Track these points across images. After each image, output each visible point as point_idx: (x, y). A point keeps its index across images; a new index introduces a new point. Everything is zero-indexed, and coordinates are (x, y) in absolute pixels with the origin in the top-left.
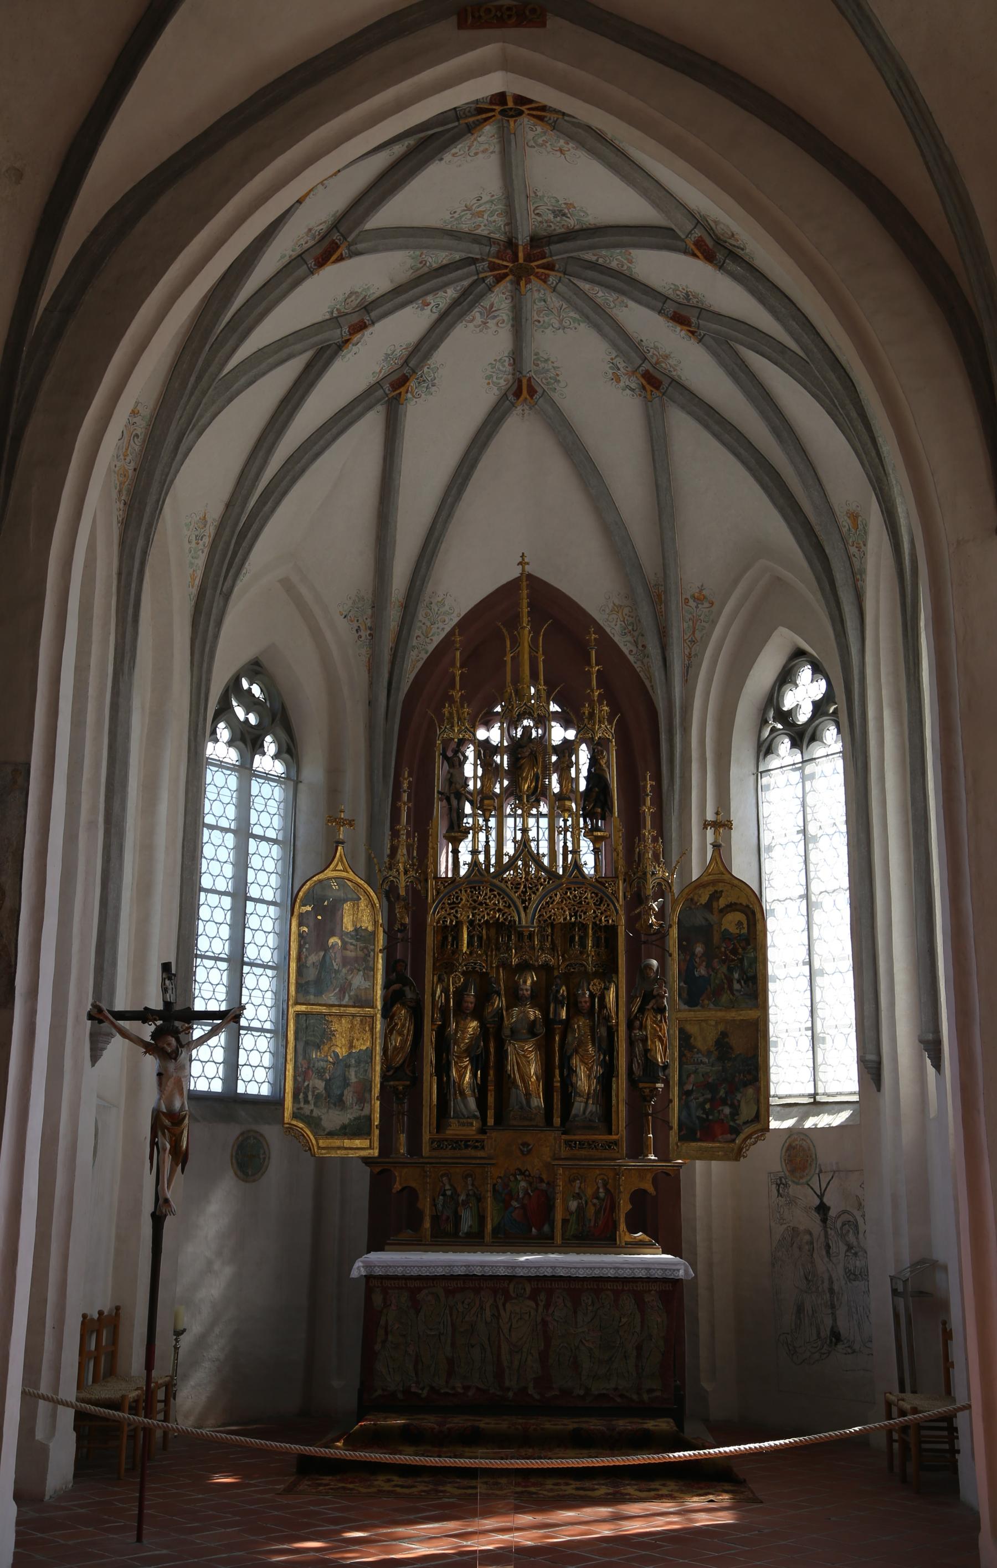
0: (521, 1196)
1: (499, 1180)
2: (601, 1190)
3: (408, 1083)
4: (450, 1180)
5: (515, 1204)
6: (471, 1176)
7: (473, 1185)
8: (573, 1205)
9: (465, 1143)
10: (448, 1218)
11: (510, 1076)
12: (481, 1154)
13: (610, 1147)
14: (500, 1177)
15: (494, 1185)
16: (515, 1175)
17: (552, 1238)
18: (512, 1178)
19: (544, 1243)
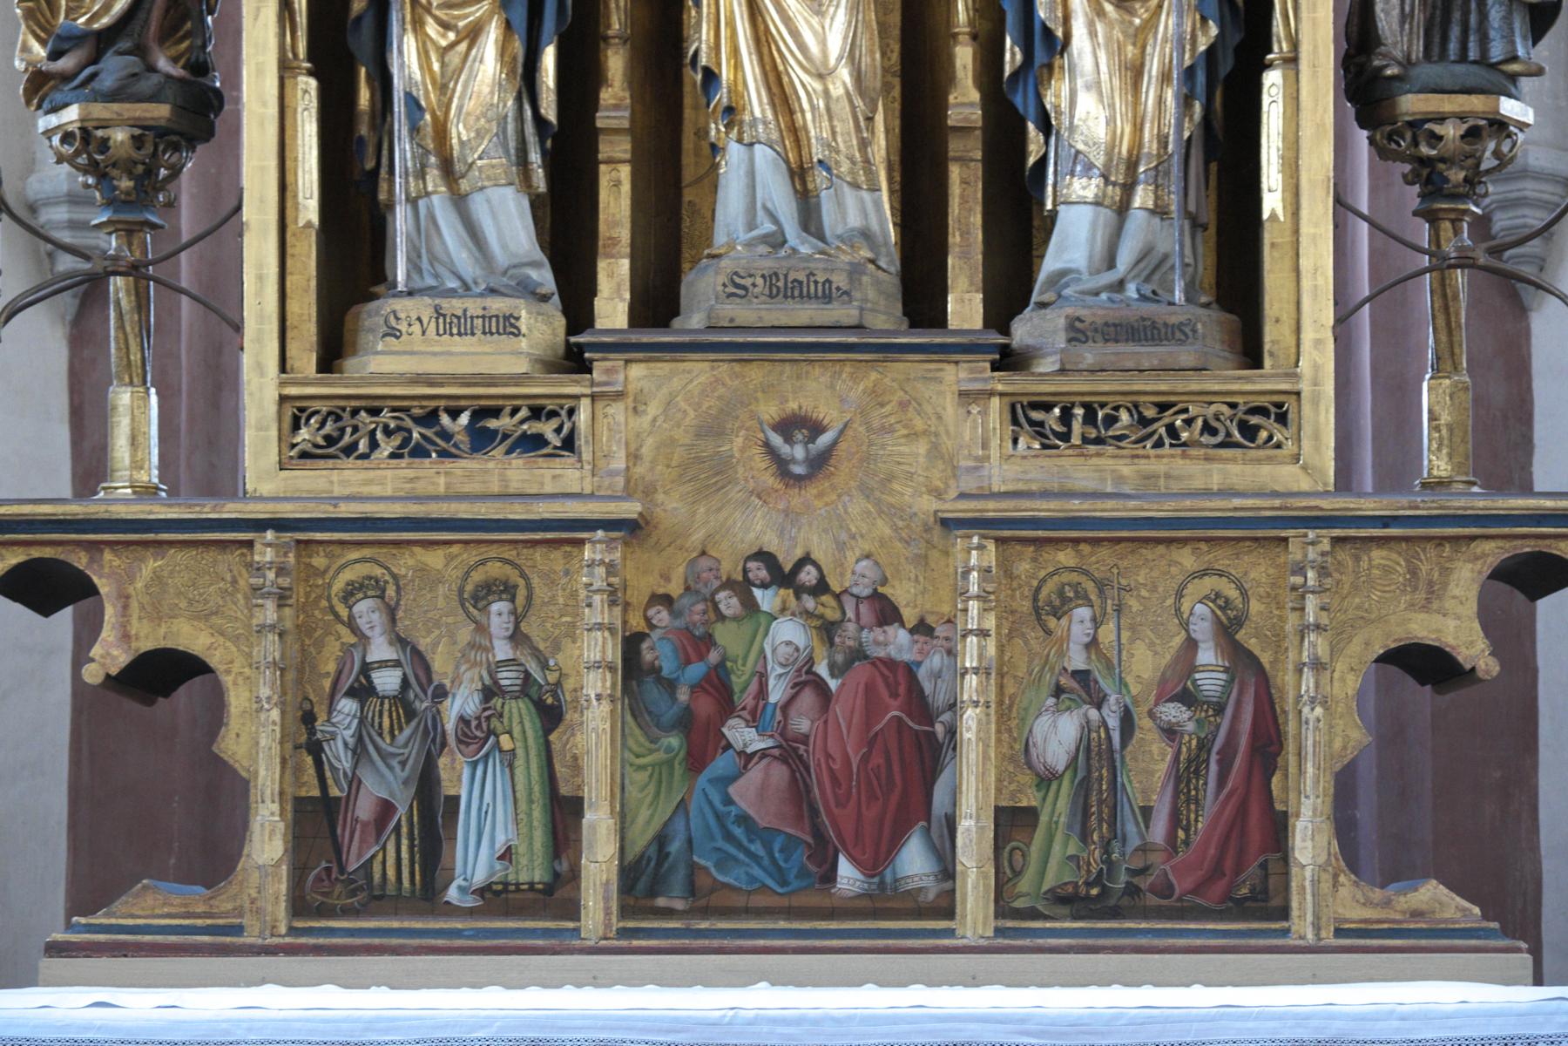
0: (777, 692)
1: (661, 616)
2: (1207, 655)
3: (160, 112)
4: (392, 613)
5: (741, 734)
6: (508, 591)
8: (1057, 736)
9: (484, 423)
10: (386, 808)
11: (711, 76)
12: (566, 475)
13: (1249, 432)
14: (666, 600)
15: (632, 644)
16: (743, 588)
18: (729, 603)
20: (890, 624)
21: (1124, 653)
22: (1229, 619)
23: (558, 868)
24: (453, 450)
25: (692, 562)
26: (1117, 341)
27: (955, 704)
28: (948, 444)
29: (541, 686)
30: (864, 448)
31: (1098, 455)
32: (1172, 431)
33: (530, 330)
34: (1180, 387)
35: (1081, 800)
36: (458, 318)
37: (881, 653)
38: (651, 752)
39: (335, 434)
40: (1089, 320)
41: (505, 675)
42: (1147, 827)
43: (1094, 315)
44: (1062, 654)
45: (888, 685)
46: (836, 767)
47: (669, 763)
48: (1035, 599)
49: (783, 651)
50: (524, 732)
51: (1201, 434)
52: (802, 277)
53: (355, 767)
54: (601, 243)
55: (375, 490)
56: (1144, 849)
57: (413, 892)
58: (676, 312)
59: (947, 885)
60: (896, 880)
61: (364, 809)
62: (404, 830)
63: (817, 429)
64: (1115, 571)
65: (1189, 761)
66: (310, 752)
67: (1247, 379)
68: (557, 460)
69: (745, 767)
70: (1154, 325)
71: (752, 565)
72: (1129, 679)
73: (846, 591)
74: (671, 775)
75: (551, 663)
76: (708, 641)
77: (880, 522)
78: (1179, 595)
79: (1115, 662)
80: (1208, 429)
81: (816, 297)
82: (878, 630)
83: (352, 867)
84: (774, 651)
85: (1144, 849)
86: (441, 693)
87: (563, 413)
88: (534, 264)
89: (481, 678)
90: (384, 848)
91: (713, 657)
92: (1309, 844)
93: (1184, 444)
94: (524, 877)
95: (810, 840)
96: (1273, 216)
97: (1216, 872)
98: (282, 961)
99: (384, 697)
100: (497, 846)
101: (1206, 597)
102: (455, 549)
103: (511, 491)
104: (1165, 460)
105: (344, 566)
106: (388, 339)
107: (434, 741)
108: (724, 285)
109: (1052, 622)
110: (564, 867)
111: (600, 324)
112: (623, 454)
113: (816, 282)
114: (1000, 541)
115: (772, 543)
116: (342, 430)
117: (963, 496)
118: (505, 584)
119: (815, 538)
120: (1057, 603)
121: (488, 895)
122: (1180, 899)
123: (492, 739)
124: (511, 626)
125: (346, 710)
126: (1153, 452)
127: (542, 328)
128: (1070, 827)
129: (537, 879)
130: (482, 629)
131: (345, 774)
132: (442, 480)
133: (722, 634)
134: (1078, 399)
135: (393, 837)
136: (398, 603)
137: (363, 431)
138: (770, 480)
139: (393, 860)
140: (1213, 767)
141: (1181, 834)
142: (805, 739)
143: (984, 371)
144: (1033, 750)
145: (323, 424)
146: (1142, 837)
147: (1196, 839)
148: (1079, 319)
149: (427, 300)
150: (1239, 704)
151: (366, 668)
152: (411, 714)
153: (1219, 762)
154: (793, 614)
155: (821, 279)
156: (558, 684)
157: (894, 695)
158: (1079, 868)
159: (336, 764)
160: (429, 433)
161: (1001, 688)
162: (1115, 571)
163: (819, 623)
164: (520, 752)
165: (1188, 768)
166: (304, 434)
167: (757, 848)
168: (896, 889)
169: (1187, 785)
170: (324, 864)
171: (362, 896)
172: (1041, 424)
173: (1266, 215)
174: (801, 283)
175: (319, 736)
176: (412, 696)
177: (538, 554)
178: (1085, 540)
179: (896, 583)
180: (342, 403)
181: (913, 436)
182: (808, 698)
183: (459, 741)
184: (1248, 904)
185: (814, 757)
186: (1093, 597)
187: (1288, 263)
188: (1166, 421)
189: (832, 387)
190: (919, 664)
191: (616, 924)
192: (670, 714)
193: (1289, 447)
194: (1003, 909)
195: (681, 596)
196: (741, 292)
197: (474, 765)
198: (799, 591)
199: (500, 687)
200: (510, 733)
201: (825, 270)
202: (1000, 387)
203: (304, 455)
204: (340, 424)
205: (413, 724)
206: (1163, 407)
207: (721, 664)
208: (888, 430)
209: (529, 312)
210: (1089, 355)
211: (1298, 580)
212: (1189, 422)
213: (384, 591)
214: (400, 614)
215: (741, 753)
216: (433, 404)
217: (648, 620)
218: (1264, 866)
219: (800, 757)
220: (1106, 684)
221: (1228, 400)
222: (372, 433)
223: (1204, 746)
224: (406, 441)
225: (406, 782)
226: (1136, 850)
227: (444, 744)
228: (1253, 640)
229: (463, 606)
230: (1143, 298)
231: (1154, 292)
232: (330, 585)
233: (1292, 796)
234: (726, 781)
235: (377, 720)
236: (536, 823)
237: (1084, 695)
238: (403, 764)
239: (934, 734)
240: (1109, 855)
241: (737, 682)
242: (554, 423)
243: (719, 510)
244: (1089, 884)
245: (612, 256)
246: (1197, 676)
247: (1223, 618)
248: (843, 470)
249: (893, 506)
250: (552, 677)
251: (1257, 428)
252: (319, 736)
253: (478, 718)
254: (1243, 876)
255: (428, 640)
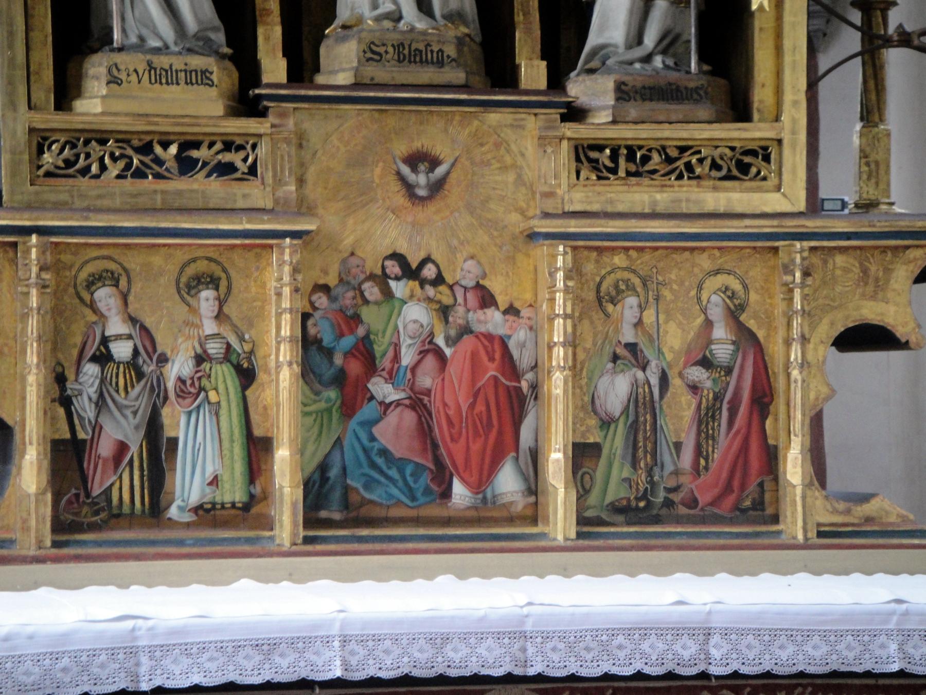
0: (408, 358)
1: (322, 300)
2: (720, 332)
5: (382, 389)
6: (214, 282)
7: (220, 317)
8: (616, 390)
10: (122, 448)
12: (255, 193)
14: (325, 289)
16: (382, 280)
17: (534, 514)
18: (372, 291)
19: (504, 532)
20: (489, 307)
21: (661, 330)
22: (735, 305)
23: (253, 491)
24: (166, 174)
25: (344, 261)
26: (651, 100)
27: (536, 365)
28: (528, 175)
29: (239, 355)
30: (469, 176)
31: (638, 184)
32: (689, 167)
33: (220, 80)
34: (697, 135)
35: (632, 438)
36: (166, 71)
37: (481, 329)
38: (315, 402)
39: (72, 159)
40: (631, 84)
41: (212, 345)
42: (678, 457)
43: (635, 80)
44: (617, 331)
45: (487, 353)
46: (451, 413)
47: (329, 410)
48: (598, 291)
49: (411, 327)
50: (227, 389)
51: (710, 170)
52: (421, 46)
53: (97, 417)
54: (257, 13)
55: (106, 203)
56: (676, 473)
57: (143, 511)
58: (317, 69)
59: (532, 499)
60: (494, 496)
61: (105, 448)
62: (136, 464)
63: (434, 163)
64: (655, 270)
65: (708, 409)
66: (62, 404)
67: (745, 130)
68: (245, 182)
69: (385, 413)
70: (678, 89)
71: (388, 263)
72: (665, 350)
73: (457, 283)
74: (330, 420)
75: (247, 337)
76: (356, 319)
77: (481, 232)
78: (700, 288)
79: (655, 336)
80: (715, 166)
81: (432, 63)
82: (480, 312)
83: (96, 492)
84: (405, 328)
85: (676, 473)
86: (163, 360)
87: (249, 147)
88: (215, 29)
89: (194, 348)
90: (120, 477)
91: (361, 331)
92: (799, 470)
93: (699, 177)
94: (228, 498)
95: (432, 467)
96: (761, 7)
97: (728, 488)
98: (49, 567)
99: (119, 363)
100: (207, 475)
101: (719, 290)
102: (171, 251)
103: (211, 206)
104: (685, 189)
105: (87, 262)
106: (112, 85)
107: (158, 395)
108: (365, 52)
109: (610, 308)
110: (257, 490)
111: (266, 79)
112: (293, 179)
113: (432, 51)
114: (575, 248)
115: (403, 247)
116: (77, 156)
117: (546, 215)
118: (211, 277)
119: (434, 243)
120: (614, 293)
121: (201, 512)
122: (702, 509)
123: (202, 394)
124: (216, 309)
125: (90, 372)
126: (677, 183)
127: (224, 76)
128: (624, 457)
129: (237, 500)
130: (194, 311)
131: (90, 421)
132: (159, 197)
133: (367, 314)
134: (623, 143)
135: (127, 469)
136: (129, 290)
137: (94, 156)
138: (400, 199)
139: (126, 487)
140: (725, 414)
141: (702, 462)
142: (428, 392)
143: (556, 121)
144: (597, 402)
145: (62, 150)
146: (675, 464)
147: (713, 466)
148: (624, 83)
149: (141, 56)
150: (742, 367)
151: (105, 341)
152: (140, 375)
153: (729, 409)
154: (419, 300)
155: (436, 49)
156: (252, 352)
157: (492, 359)
158: (631, 487)
159: (82, 414)
160: (147, 160)
161: (574, 354)
162: (655, 270)
163: (437, 307)
164: (224, 404)
165: (707, 414)
166: (47, 157)
167: (393, 473)
168: (494, 503)
169: (707, 426)
170: (74, 491)
171: (103, 515)
172: (597, 161)
173: (754, 7)
174: (421, 52)
175: (69, 392)
176: (141, 361)
177: (236, 256)
178: (633, 248)
179: (493, 277)
180: (77, 135)
181: (504, 168)
182: (430, 362)
183: (178, 396)
184: (751, 512)
185: (435, 404)
186: (639, 290)
187: (770, 44)
188: (686, 160)
189: (446, 130)
190: (509, 337)
191: (302, 533)
192: (329, 373)
193: (773, 180)
194: (582, 521)
195: (336, 286)
196: (376, 57)
197: (189, 414)
198: (423, 283)
199: (208, 355)
200: (216, 389)
201: (439, 42)
202: (569, 134)
203: (48, 174)
204: (75, 151)
205: (143, 383)
206: (683, 149)
207: (367, 336)
208: (488, 164)
209: (219, 68)
210: (633, 110)
211: (789, 278)
212: (701, 161)
213: (118, 281)
214: (131, 298)
215: (381, 403)
216: (148, 138)
217: (312, 304)
218: (761, 485)
219: (425, 406)
220: (649, 353)
221: (730, 144)
222: (101, 160)
223: (718, 397)
224: (129, 166)
225: (137, 428)
226: (671, 473)
227: (166, 398)
228: (752, 321)
229: (179, 292)
230: (666, 67)
231: (676, 64)
232: (76, 277)
233: (782, 435)
234: (369, 424)
235: (114, 380)
236: (236, 457)
237: (633, 361)
238: (135, 413)
239: (520, 388)
240: (652, 477)
241: (378, 350)
242: (242, 154)
243: (363, 222)
244: (638, 499)
245: (268, 24)
246: (713, 347)
247: (732, 307)
248: (454, 191)
249: (490, 220)
250: (247, 347)
251: (749, 165)
252: (69, 392)
253: (192, 378)
254: (746, 493)
255: (153, 319)
